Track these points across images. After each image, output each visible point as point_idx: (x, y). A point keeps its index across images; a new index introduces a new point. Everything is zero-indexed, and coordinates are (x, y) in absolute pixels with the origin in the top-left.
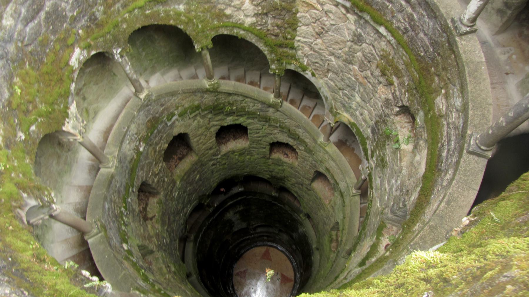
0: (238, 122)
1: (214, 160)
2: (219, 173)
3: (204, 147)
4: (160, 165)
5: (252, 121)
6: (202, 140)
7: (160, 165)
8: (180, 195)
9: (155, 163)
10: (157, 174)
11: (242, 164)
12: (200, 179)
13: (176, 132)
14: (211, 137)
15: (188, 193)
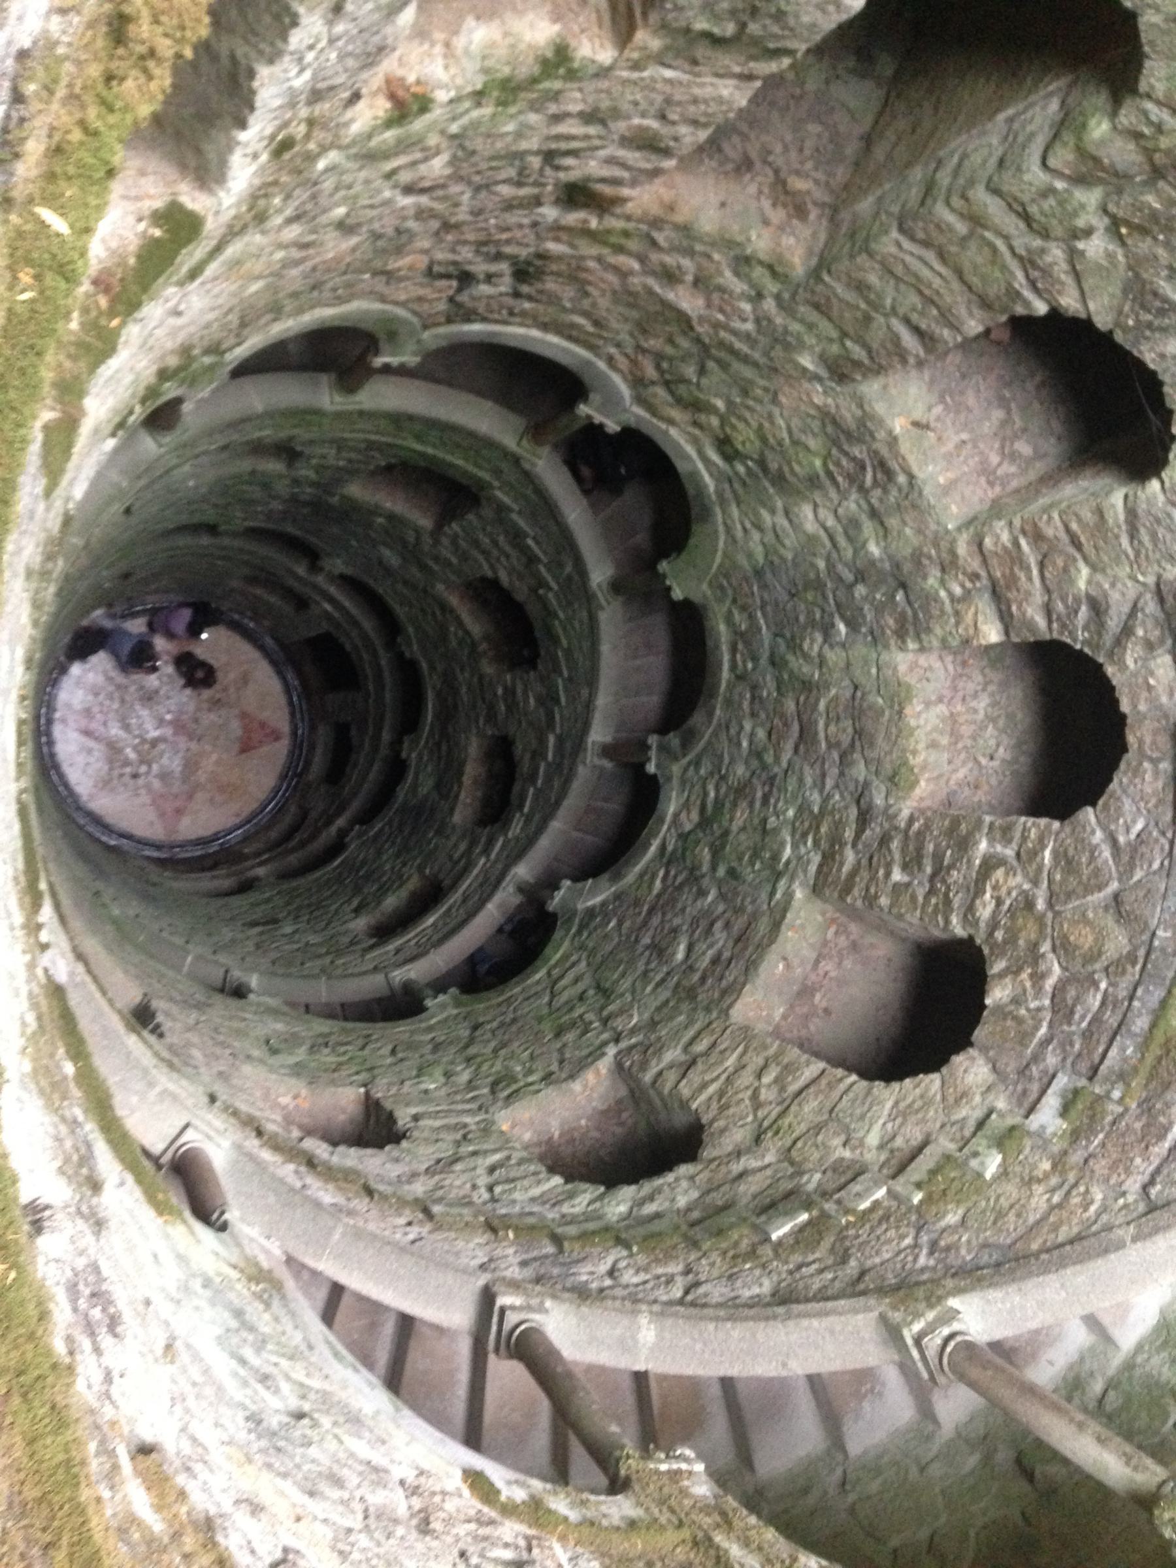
0: (628, 1192)
1: (633, 1032)
2: (565, 997)
3: (731, 1061)
4: (985, 911)
5: (566, 1209)
6: (766, 1080)
7: (985, 911)
8: (756, 855)
9: (1030, 904)
10: (990, 864)
11: (472, 1050)
12: (660, 950)
13: (971, 1069)
14: (723, 1108)
15: (705, 882)
